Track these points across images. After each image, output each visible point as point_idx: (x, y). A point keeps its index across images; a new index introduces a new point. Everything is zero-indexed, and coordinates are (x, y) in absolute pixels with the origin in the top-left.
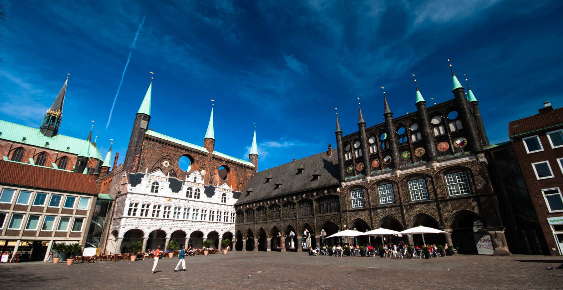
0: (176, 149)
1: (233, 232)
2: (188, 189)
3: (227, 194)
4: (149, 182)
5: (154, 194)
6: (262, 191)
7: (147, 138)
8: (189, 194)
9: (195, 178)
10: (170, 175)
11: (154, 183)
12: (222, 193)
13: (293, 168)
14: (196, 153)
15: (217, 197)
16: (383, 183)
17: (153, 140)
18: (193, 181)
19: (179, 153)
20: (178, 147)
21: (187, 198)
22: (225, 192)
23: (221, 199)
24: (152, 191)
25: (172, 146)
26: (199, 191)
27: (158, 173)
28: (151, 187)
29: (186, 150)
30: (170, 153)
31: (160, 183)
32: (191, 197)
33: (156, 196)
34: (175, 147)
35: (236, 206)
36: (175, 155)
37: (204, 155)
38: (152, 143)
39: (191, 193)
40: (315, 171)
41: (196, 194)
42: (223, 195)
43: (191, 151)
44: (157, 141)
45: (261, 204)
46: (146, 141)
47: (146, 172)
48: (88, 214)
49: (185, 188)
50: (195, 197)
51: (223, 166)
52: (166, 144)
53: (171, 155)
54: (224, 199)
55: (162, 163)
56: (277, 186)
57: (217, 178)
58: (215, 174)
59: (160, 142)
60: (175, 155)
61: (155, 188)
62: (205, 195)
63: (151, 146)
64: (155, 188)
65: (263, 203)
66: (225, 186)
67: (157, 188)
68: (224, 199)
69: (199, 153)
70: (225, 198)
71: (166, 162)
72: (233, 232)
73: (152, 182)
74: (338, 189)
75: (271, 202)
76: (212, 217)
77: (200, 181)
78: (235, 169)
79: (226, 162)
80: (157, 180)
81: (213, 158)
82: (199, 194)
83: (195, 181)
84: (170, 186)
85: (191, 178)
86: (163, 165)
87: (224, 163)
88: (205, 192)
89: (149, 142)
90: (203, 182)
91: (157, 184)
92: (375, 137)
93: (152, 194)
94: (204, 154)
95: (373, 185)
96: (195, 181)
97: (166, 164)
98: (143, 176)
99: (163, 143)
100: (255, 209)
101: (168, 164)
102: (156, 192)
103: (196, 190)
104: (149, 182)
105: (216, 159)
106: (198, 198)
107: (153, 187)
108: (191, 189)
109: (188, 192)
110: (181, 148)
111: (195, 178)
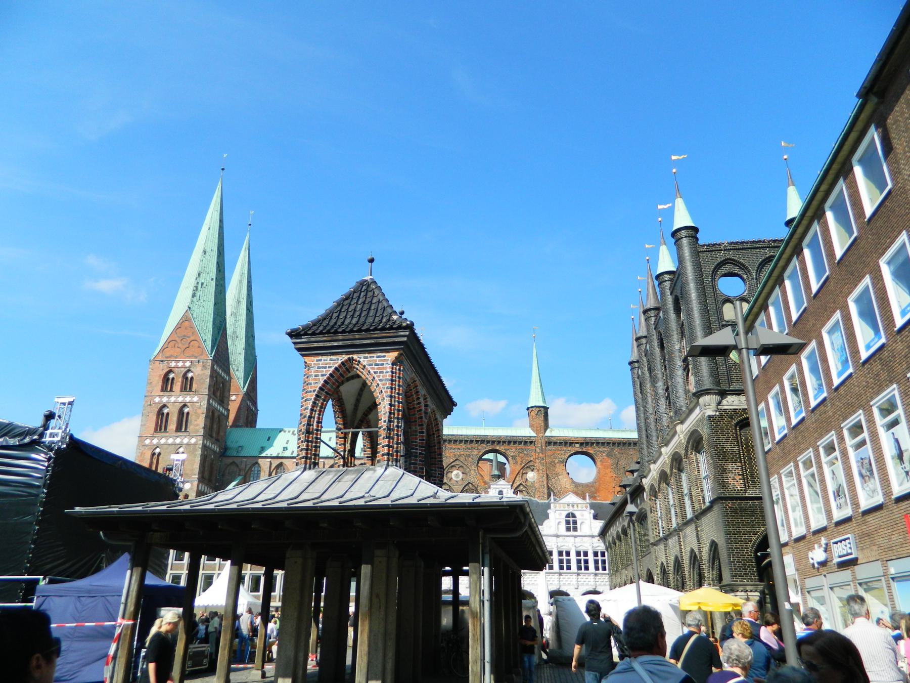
0: (468, 445)
3: (577, 514)
12: (565, 513)
14: (509, 442)
20: (472, 441)
22: (571, 510)
23: (563, 526)
25: (461, 441)
29: (488, 442)
30: (460, 456)
34: (466, 441)
36: (469, 456)
37: (526, 442)
42: (568, 516)
43: (499, 442)
53: (462, 459)
55: (449, 475)
58: (557, 475)
60: (469, 456)
69: (515, 442)
70: (575, 523)
71: (455, 472)
78: (609, 455)
79: (582, 444)
81: (549, 443)
86: (451, 479)
94: (526, 442)
97: (457, 475)
105: (555, 443)
110: (477, 441)
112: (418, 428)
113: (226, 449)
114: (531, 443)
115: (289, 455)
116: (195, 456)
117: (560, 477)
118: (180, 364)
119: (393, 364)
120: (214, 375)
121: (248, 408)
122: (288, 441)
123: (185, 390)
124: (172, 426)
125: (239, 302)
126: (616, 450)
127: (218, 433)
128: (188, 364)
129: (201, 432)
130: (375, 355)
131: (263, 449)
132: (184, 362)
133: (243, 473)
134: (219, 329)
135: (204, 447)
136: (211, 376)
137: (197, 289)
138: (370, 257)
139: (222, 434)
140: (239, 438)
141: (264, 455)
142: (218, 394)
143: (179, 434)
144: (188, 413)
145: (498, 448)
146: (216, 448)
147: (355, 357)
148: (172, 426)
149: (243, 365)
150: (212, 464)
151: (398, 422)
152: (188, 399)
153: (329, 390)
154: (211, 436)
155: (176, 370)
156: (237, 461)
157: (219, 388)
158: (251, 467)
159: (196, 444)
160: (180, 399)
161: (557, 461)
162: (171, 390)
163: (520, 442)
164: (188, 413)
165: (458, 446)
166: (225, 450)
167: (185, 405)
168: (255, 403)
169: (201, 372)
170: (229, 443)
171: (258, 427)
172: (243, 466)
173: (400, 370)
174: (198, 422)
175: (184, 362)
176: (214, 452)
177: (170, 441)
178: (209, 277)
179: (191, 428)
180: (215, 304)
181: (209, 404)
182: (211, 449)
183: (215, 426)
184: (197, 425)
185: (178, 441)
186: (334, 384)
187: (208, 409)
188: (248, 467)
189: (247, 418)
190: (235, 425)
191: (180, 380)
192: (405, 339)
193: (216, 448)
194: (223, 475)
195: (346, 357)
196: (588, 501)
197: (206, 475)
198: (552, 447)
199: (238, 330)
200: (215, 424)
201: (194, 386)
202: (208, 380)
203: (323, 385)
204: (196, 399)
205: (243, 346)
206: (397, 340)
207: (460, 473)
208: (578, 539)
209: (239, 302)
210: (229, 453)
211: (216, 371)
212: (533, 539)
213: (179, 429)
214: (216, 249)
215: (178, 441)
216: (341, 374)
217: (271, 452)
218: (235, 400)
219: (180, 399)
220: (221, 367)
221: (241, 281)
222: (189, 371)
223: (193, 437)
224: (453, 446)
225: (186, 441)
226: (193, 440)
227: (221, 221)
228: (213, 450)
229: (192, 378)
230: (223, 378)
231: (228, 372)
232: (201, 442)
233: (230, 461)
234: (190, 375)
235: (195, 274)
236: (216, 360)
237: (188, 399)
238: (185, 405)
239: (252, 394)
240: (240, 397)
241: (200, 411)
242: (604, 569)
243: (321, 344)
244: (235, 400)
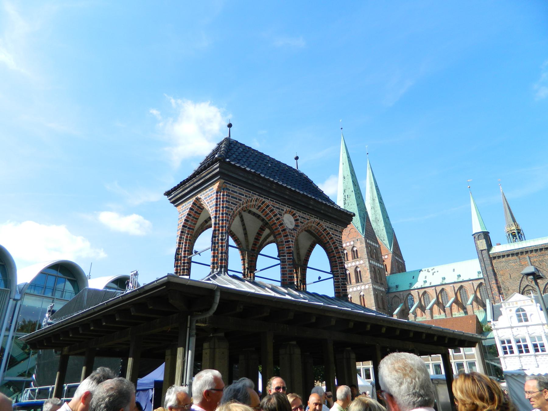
0: (539, 253)
7: (495, 258)
11: (518, 311)
17: (504, 256)
20: (541, 250)
24: (520, 321)
33: (527, 326)
36: (542, 261)
38: (504, 259)
44: (508, 255)
48: (476, 356)
59: (513, 255)
60: (542, 261)
63: (503, 264)
67: (525, 315)
80: (519, 305)
93: (521, 324)
98: (501, 307)
104: (511, 310)
107: (519, 316)
112: (284, 239)
113: (389, 288)
115: (429, 285)
116: (370, 296)
118: (348, 244)
119: (217, 193)
120: (368, 245)
121: (397, 261)
122: (426, 277)
123: (355, 258)
124: (353, 280)
125: (374, 200)
127: (381, 279)
128: (352, 243)
129: (370, 281)
130: (208, 190)
131: (411, 284)
132: (350, 242)
133: (403, 301)
134: (364, 218)
135: (374, 289)
136: (367, 247)
137: (345, 199)
138: (227, 124)
139: (383, 280)
140: (398, 281)
141: (413, 288)
142: (374, 257)
143: (358, 284)
144: (360, 271)
146: (382, 289)
147: (199, 196)
148: (353, 280)
149: (386, 236)
150: (382, 299)
151: (222, 236)
152: (357, 263)
153: (190, 225)
154: (377, 282)
155: (347, 248)
156: (397, 294)
157: (374, 253)
158: (407, 297)
159: (369, 288)
160: (354, 264)
162: (347, 260)
164: (360, 271)
166: (388, 290)
167: (357, 267)
168: (401, 257)
169: (360, 246)
170: (390, 285)
171: (407, 270)
172: (402, 297)
173: (223, 195)
174: (367, 275)
175: (350, 242)
176: (382, 292)
177: (355, 289)
178: (350, 191)
179: (363, 279)
180: (358, 205)
181: (370, 263)
182: (379, 290)
183: (378, 276)
184: (367, 277)
185: (359, 288)
186: (192, 220)
187: (370, 267)
188: (405, 297)
189: (398, 267)
190: (392, 273)
191: (350, 253)
192: (218, 170)
193: (382, 289)
194: (392, 305)
195: (194, 198)
197: (381, 306)
199: (378, 216)
200: (378, 275)
201: (359, 255)
202: (365, 249)
203: (185, 223)
204: (362, 262)
205: (383, 225)
206: (214, 173)
209: (374, 200)
210: (391, 291)
211: (369, 243)
212: (344, 317)
213: (357, 281)
214: (349, 174)
215: (359, 288)
216: (196, 212)
217: (418, 285)
218: (387, 258)
219: (354, 264)
220: (371, 240)
221: (371, 188)
222: (354, 247)
223: (366, 284)
225: (363, 287)
226: (367, 287)
227: (349, 157)
228: (381, 291)
229: (357, 250)
230: (375, 246)
231: (377, 242)
232: (371, 287)
233: (393, 295)
234: (355, 249)
235: (343, 192)
236: (366, 237)
237: (357, 263)
238: (357, 267)
239: (397, 252)
240: (391, 255)
241: (366, 269)
243: (181, 195)
244: (387, 258)
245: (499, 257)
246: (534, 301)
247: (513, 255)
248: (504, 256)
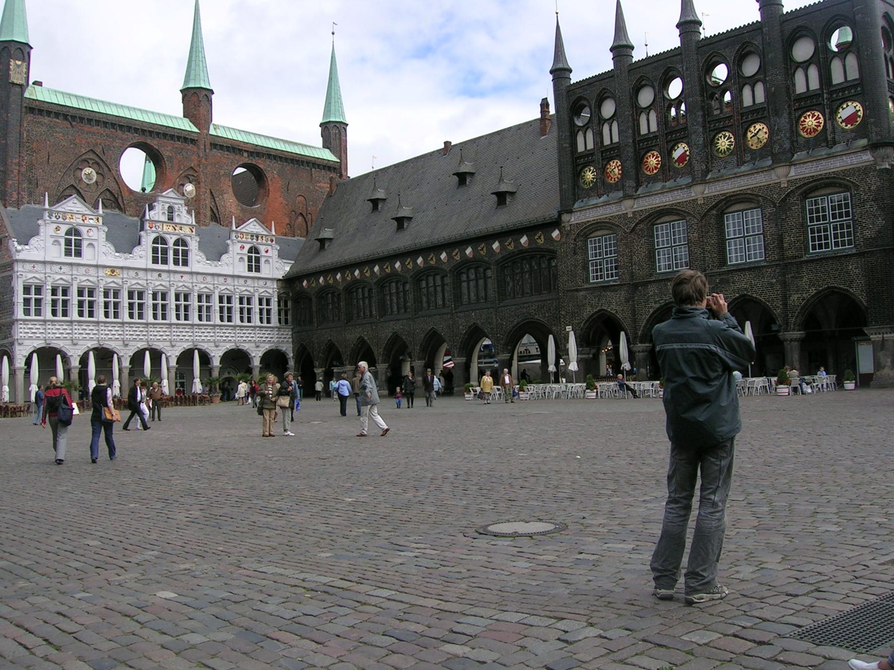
1: (288, 348)
2: (155, 241)
3: (262, 249)
4: (57, 229)
5: (73, 259)
6: (359, 240)
8: (159, 256)
9: (171, 210)
10: (105, 206)
11: (68, 233)
12: (247, 247)
13: (452, 165)
15: (234, 262)
16: (667, 218)
17: (49, 113)
18: (164, 218)
19: (117, 143)
20: (113, 125)
21: (156, 266)
25: (98, 122)
26: (185, 244)
27: (73, 205)
28: (63, 242)
29: (136, 130)
31: (84, 230)
32: (165, 261)
35: (289, 282)
37: (186, 139)
38: (46, 120)
39: (165, 252)
40: (501, 180)
41: (176, 252)
44: (57, 115)
45: (357, 273)
46: (30, 117)
47: (47, 206)
49: (148, 239)
50: (176, 262)
51: (242, 166)
52: (82, 119)
53: (98, 151)
54: (254, 264)
56: (401, 222)
57: (229, 202)
59: (65, 117)
61: (73, 244)
62: (201, 257)
63: (44, 129)
64: (73, 244)
65: (361, 272)
66: (253, 226)
67: (79, 244)
68: (254, 264)
70: (258, 260)
71: (88, 170)
72: (288, 348)
73: (64, 229)
74: (555, 234)
75: (381, 269)
76: (226, 314)
77: (184, 217)
81: (214, 145)
82: (185, 253)
83: (171, 219)
84: (109, 238)
85: (157, 214)
86: (81, 179)
87: (245, 158)
88: (201, 247)
89: (40, 118)
90: (192, 220)
91: (78, 233)
92: (654, 88)
95: (641, 221)
96: (171, 219)
99: (74, 117)
100: (341, 288)
101: (95, 177)
102: (79, 254)
103: (176, 243)
104: (57, 229)
105: (222, 147)
106: (185, 263)
107: (68, 243)
108: (164, 241)
109: (155, 250)
110: (121, 127)
111: (171, 210)
114: (193, 141)
117: (226, 196)
126: (288, 167)
145: (149, 142)
161: (222, 172)
163: (179, 138)
165: (95, 129)
196: (274, 233)
198: (216, 153)
207: (94, 173)
208: (261, 283)
224: (87, 128)
242: (286, 322)
245: (41, 112)
246: (101, 219)
247: (65, 117)
248: (49, 113)
